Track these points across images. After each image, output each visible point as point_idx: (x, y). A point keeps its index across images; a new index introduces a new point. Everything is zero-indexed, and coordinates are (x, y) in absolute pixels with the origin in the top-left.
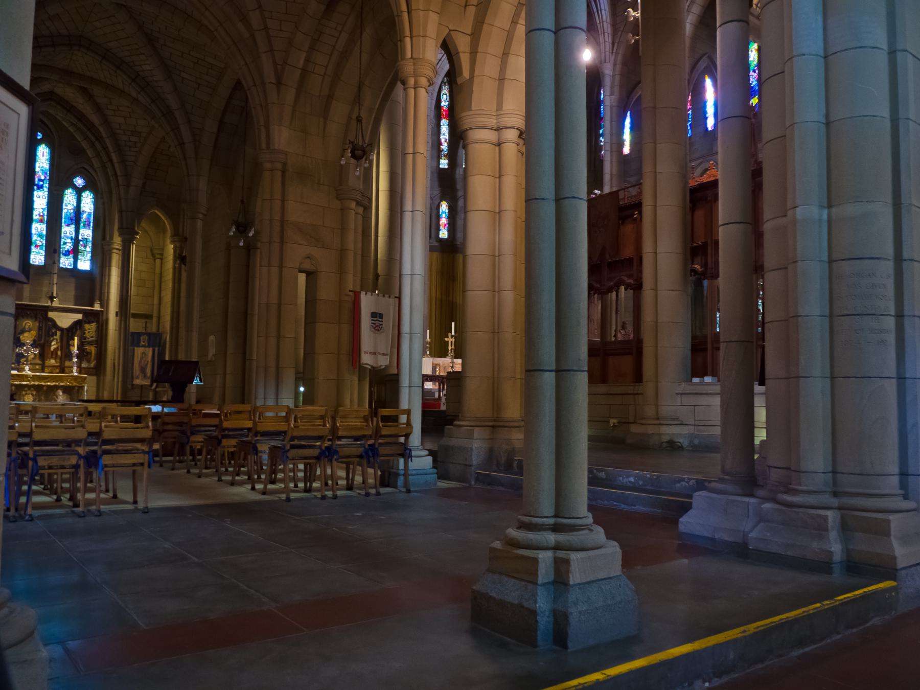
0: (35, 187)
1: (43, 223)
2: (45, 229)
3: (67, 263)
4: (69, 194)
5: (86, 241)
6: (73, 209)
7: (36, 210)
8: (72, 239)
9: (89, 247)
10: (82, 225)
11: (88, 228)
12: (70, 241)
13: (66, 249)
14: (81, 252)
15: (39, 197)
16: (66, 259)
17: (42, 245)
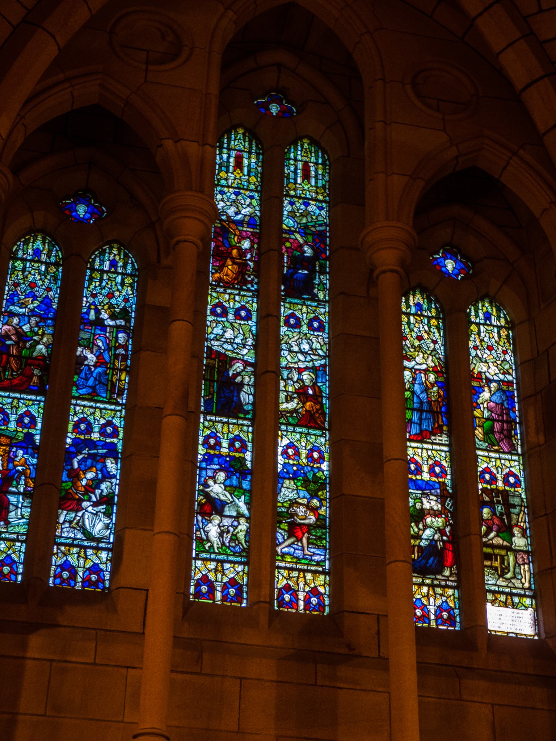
0: (283, 288)
1: (322, 428)
2: (326, 455)
3: (432, 609)
4: (413, 310)
5: (508, 506)
6: (435, 370)
7: (285, 374)
8: (442, 497)
9: (524, 535)
10: (479, 432)
11: (504, 446)
12: (437, 507)
13: (423, 543)
14: (488, 557)
15: (298, 325)
16: (425, 589)
17: (319, 518)
